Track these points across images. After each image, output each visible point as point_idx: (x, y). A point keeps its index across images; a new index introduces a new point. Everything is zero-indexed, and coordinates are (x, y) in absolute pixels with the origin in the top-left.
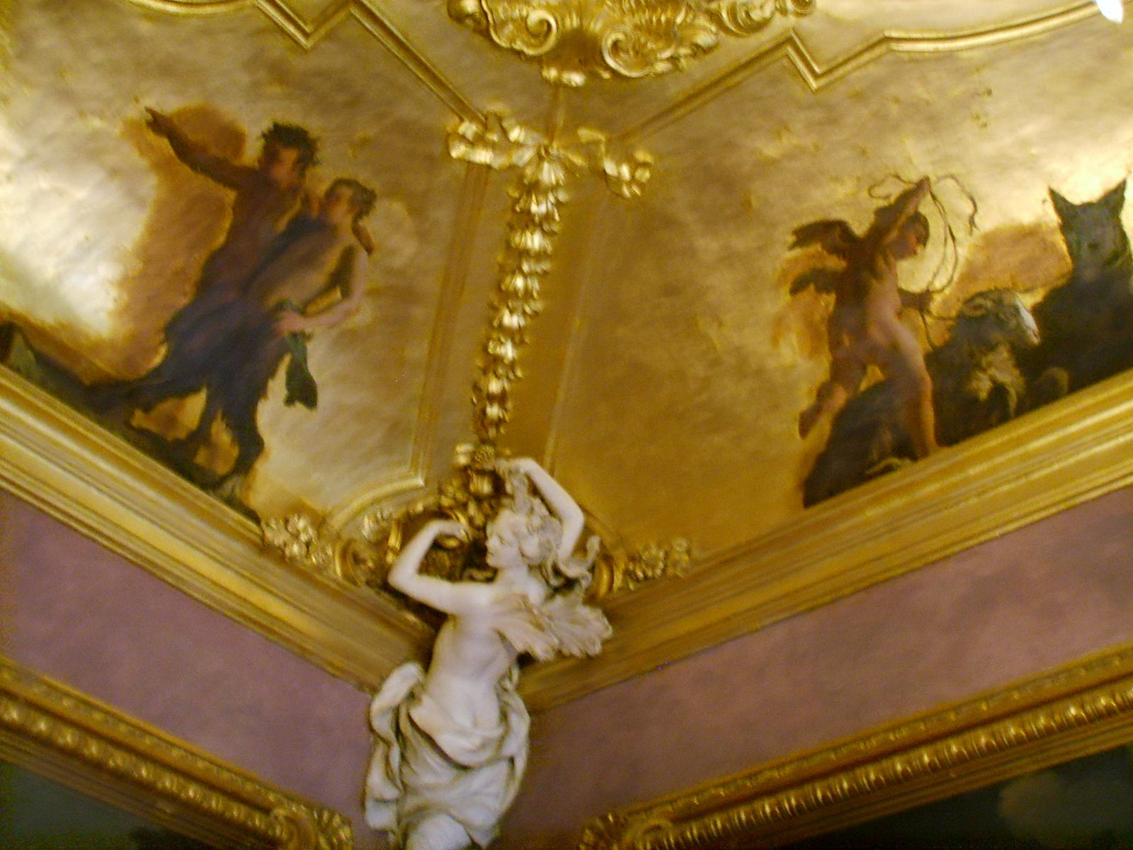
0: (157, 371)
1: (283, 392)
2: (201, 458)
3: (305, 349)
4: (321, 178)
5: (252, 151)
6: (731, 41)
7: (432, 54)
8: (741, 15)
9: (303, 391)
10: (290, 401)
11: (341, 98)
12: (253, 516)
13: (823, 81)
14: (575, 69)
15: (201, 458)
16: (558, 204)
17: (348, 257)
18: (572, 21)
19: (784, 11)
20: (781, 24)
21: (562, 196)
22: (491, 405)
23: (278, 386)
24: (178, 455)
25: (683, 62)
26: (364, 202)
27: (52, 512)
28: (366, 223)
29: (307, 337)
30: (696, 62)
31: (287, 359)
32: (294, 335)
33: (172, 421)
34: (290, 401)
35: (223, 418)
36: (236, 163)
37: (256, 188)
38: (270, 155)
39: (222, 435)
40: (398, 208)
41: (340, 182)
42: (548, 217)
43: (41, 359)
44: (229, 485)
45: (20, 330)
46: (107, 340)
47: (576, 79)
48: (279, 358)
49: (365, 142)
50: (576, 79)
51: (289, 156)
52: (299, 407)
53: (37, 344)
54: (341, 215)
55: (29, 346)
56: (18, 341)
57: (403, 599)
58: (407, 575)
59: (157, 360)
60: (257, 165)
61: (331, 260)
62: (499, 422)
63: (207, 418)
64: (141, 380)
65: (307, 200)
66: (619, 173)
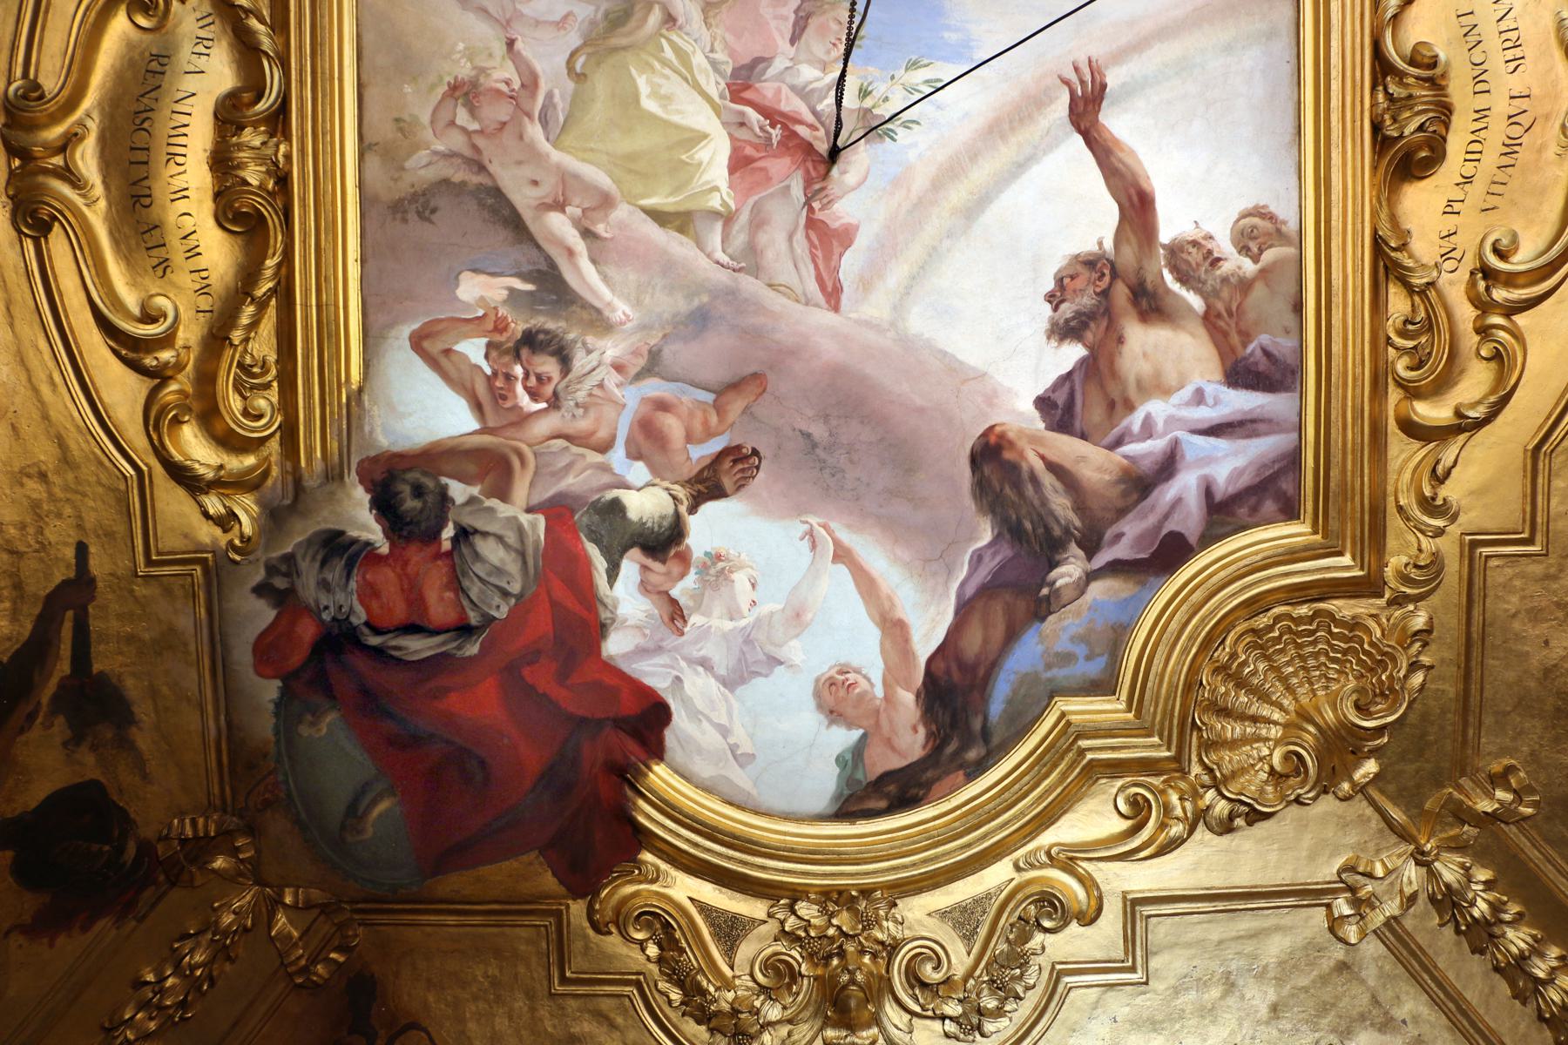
6: (1435, 599)
7: (1244, 877)
8: (1414, 574)
11: (1215, 993)
13: (1539, 537)
14: (1357, 765)
16: (1489, 885)
18: (1309, 733)
19: (1439, 532)
20: (1448, 545)
21: (1483, 875)
25: (1425, 659)
30: (1433, 647)
42: (1496, 908)
47: (1370, 767)
49: (1274, 1008)
50: (1370, 767)
66: (1499, 801)
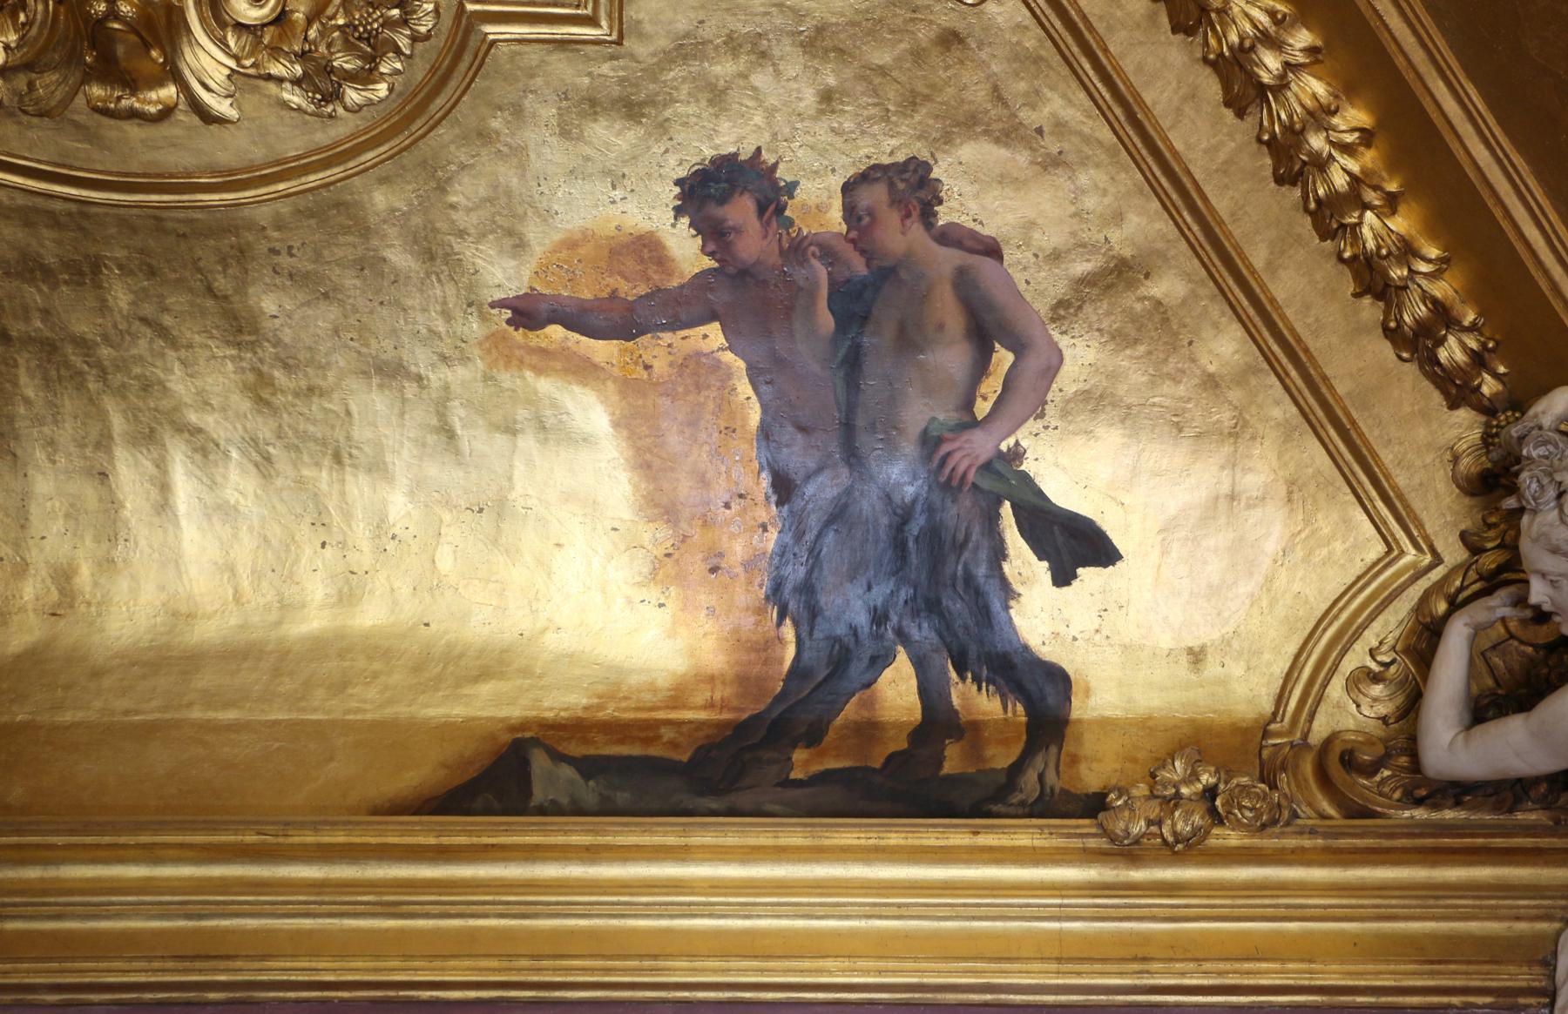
0: (798, 671)
1: (1042, 569)
2: (953, 761)
3: (1026, 479)
4: (819, 202)
5: (686, 250)
9: (1076, 546)
10: (1063, 577)
12: (1094, 805)
15: (953, 761)
17: (964, 283)
22: (1441, 342)
23: (1024, 564)
24: (917, 783)
26: (912, 186)
27: (701, 995)
28: (945, 215)
29: (1017, 454)
31: (1006, 509)
32: (987, 467)
33: (869, 730)
34: (1063, 577)
35: (961, 671)
36: (675, 283)
37: (743, 292)
38: (714, 234)
39: (980, 702)
40: (972, 151)
41: (847, 188)
43: (590, 767)
44: (1030, 778)
45: (536, 742)
46: (726, 667)
48: (993, 519)
51: (741, 211)
52: (1088, 576)
53: (575, 749)
54: (899, 236)
55: (558, 757)
56: (539, 762)
57: (1506, 792)
58: (1446, 744)
59: (790, 652)
60: (709, 263)
61: (948, 311)
62: (1479, 360)
63: (930, 691)
64: (779, 698)
65: (828, 253)
